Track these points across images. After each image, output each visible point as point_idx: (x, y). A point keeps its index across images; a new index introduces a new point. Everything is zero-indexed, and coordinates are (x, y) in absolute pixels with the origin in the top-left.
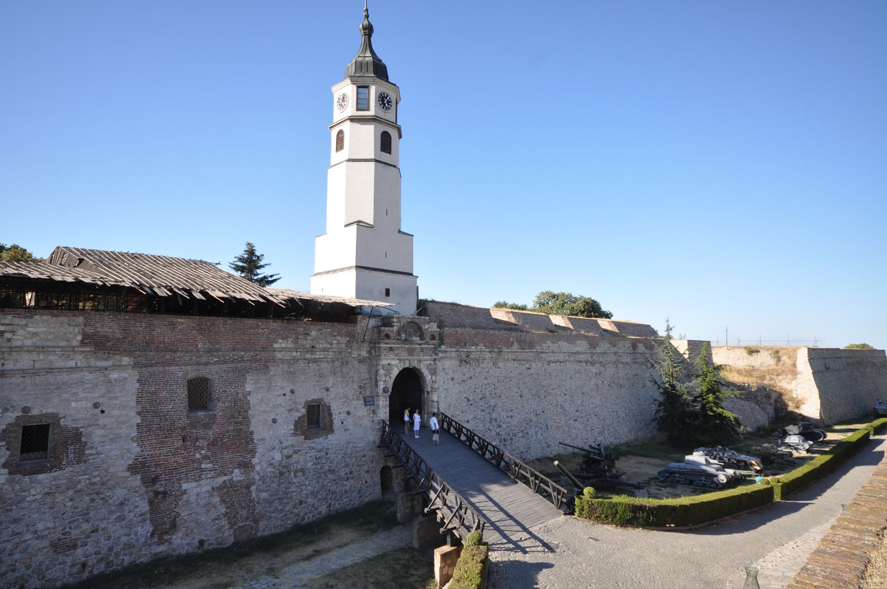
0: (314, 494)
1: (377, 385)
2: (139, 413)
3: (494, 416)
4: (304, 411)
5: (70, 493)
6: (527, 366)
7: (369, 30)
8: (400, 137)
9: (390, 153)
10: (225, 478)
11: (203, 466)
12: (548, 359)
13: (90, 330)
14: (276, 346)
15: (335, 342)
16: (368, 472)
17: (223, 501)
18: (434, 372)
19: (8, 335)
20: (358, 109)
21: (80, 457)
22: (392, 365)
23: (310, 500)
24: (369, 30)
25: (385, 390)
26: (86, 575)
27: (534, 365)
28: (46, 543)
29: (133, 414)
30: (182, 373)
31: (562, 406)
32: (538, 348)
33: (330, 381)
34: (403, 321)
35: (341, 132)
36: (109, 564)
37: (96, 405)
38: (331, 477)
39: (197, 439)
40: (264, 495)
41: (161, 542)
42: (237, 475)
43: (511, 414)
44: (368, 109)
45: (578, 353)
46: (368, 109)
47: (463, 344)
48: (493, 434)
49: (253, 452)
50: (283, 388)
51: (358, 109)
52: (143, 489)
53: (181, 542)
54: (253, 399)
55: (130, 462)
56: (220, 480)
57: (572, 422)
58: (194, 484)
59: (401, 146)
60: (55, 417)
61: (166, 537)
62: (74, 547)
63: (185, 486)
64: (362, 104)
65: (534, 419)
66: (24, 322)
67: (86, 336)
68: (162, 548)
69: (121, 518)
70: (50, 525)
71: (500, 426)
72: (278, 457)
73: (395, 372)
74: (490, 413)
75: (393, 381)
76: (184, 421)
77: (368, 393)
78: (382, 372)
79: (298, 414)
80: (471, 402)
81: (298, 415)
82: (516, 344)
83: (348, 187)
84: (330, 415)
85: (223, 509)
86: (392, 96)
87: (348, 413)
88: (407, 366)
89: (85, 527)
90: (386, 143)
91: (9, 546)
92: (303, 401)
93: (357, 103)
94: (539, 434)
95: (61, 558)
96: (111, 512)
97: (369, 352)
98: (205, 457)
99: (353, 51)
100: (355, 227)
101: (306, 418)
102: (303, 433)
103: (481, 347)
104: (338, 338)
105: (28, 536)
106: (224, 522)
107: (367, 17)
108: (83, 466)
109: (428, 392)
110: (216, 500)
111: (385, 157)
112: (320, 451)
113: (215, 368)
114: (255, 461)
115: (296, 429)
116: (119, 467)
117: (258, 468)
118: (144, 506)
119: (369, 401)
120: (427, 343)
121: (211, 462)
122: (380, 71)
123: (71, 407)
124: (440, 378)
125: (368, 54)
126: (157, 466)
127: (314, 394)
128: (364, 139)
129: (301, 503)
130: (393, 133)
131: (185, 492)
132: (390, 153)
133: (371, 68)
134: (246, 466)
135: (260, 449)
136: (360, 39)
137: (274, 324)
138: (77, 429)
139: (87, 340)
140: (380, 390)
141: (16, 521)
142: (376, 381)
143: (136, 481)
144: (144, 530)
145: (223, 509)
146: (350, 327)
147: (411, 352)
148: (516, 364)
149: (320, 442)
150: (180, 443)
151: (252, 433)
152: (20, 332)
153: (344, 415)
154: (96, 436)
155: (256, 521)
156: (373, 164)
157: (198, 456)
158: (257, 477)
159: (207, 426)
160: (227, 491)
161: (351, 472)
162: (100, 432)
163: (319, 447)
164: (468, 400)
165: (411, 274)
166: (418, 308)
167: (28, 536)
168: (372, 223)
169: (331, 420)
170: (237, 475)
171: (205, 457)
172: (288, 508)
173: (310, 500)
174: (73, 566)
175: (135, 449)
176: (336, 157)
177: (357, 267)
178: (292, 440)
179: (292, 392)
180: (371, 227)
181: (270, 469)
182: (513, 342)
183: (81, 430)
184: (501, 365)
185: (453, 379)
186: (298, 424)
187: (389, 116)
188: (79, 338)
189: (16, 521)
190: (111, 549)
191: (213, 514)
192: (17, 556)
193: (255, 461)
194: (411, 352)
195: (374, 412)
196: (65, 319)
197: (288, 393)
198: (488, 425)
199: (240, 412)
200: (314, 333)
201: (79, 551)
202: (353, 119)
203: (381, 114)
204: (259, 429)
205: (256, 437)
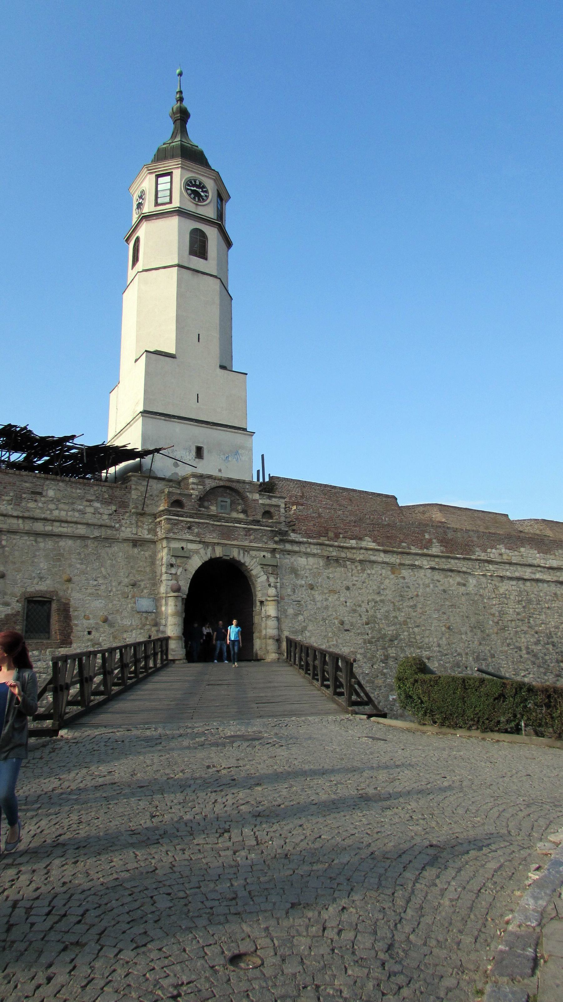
4: (17, 606)
6: (459, 579)
9: (206, 259)
15: (90, 510)
20: (157, 204)
34: (210, 484)
44: (171, 202)
47: (331, 534)
73: (196, 563)
74: (384, 648)
75: (190, 576)
79: (8, 610)
80: (347, 627)
88: (219, 552)
92: (18, 591)
101: (19, 618)
104: (97, 505)
109: (262, 602)
111: (197, 263)
120: (257, 522)
132: (206, 259)
147: (227, 533)
164: (342, 623)
168: (172, 351)
176: (131, 273)
177: (145, 413)
182: (430, 541)
194: (227, 533)
203: (190, 207)
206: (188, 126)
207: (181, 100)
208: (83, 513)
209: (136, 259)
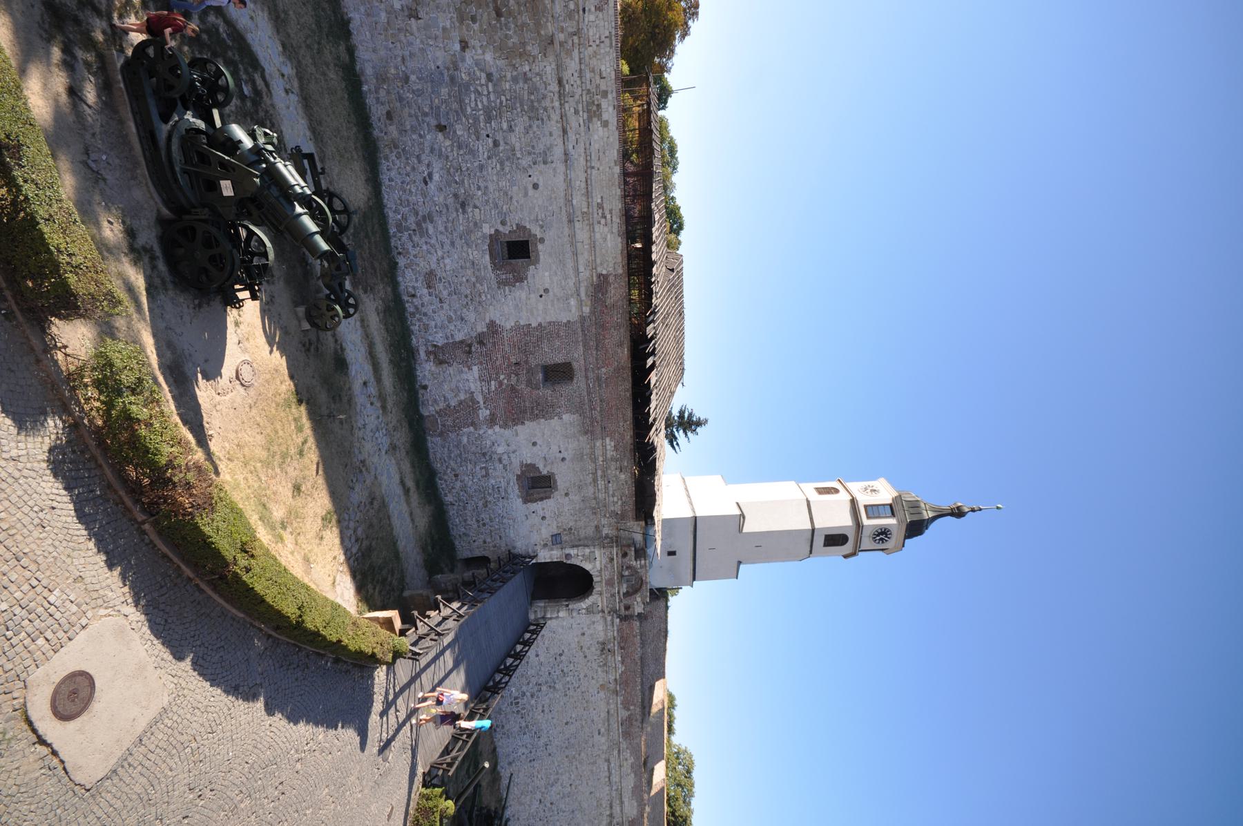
0: (464, 488)
1: (573, 547)
2: (540, 325)
3: (544, 688)
4: (545, 472)
5: (473, 279)
6: (603, 730)
7: (958, 513)
8: (845, 557)
9: (825, 545)
12: (612, 760)
13: (611, 279)
14: (608, 440)
16: (485, 542)
17: (461, 403)
18: (589, 611)
19: (603, 221)
20: (866, 507)
21: (502, 284)
22: (595, 562)
23: (458, 484)
24: (958, 513)
25: (568, 556)
26: (405, 298)
27: (603, 740)
28: (434, 266)
29: (539, 320)
30: (577, 356)
31: (557, 781)
32: (624, 745)
33: (575, 498)
34: (641, 572)
35: (837, 491)
36: (413, 314)
37: (546, 291)
38: (480, 504)
39: (517, 375)
40: (465, 440)
41: (428, 353)
42: (484, 413)
43: (547, 710)
44: (868, 517)
45: (622, 802)
46: (868, 517)
48: (524, 688)
49: (505, 426)
50: (566, 450)
51: (866, 507)
52: (474, 335)
53: (426, 370)
54: (555, 422)
56: (480, 399)
57: (538, 796)
58: (477, 376)
59: (833, 558)
60: (537, 261)
61: (432, 357)
62: (429, 287)
63: (475, 368)
64: (872, 510)
65: (542, 741)
66: (615, 230)
67: (606, 277)
68: (422, 355)
69: (450, 320)
70: (448, 268)
71: (532, 696)
72: (500, 450)
73: (587, 566)
76: (533, 362)
77: (565, 538)
78: (587, 551)
81: (541, 467)
82: (627, 714)
83: (778, 505)
84: (542, 499)
85: (453, 404)
86: (890, 544)
87: (543, 518)
88: (595, 579)
89: (445, 293)
90: (835, 540)
91: (433, 241)
92: (555, 471)
93: (872, 506)
94: (524, 750)
95: (421, 279)
96: (455, 311)
97: (607, 537)
98: (501, 383)
99: (931, 498)
100: (738, 513)
102: (523, 472)
103: (621, 668)
105: (440, 253)
106: (442, 405)
107: (973, 510)
108: (495, 286)
110: (462, 397)
111: (819, 540)
112: (506, 491)
113: (583, 385)
114: (497, 428)
115: (527, 465)
116: (493, 314)
117: (490, 432)
118: (459, 337)
119: (556, 540)
120: (621, 601)
122: (916, 528)
123: (544, 272)
124: (584, 619)
125: (931, 514)
126: (494, 344)
127: (562, 482)
128: (835, 516)
129: (456, 476)
130: (847, 548)
131: (470, 369)
132: (825, 545)
133: (915, 518)
134: (492, 421)
135: (507, 432)
136: (946, 504)
137: (628, 436)
140: (567, 551)
141: (453, 244)
142: (577, 546)
143: (481, 328)
144: (439, 339)
145: (453, 404)
146: (631, 514)
147: (610, 583)
148: (604, 715)
149: (514, 491)
150: (513, 360)
152: (606, 229)
153: (541, 513)
154: (520, 293)
155: (441, 434)
156: (810, 527)
157: (502, 377)
158: (481, 432)
159: (529, 383)
160: (470, 405)
161: (484, 525)
162: (524, 296)
163: (510, 490)
165: (694, 579)
166: (659, 590)
167: (440, 253)
169: (536, 501)
170: (484, 413)
171: (501, 383)
172: (452, 463)
173: (458, 484)
174: (414, 288)
175: (509, 325)
176: (809, 489)
178: (516, 463)
179: (563, 459)
180: (740, 530)
181: (489, 443)
184: (602, 694)
185: (583, 634)
186: (532, 467)
187: (866, 543)
188: (604, 272)
189: (453, 244)
190: (425, 314)
191: (449, 395)
192: (425, 247)
193: (497, 428)
194: (610, 583)
195: (545, 545)
196: (619, 259)
197: (561, 456)
198: (534, 681)
199: (542, 411)
200: (623, 476)
201: (425, 291)
202: (853, 502)
203: (866, 533)
204: (526, 431)
205: (519, 428)
206: (949, 517)
209: (822, 491)
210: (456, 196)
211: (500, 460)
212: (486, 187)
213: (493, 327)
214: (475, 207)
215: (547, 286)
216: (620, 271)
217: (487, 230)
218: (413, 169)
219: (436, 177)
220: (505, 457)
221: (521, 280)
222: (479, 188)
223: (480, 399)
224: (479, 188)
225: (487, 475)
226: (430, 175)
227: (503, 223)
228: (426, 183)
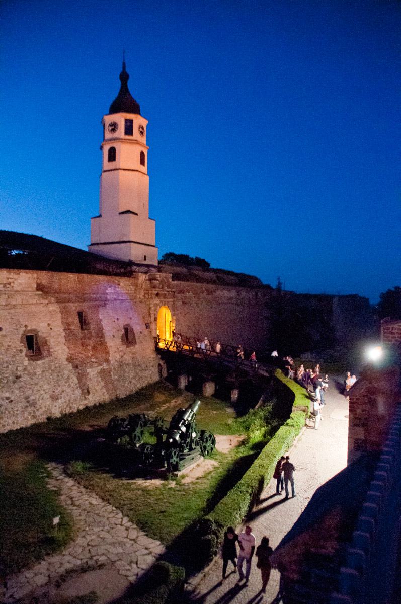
10: (101, 367)
11: (92, 360)
19: (12, 284)
21: (49, 354)
24: (124, 77)
29: (62, 330)
39: (87, 346)
40: (116, 377)
49: (108, 353)
55: (66, 357)
56: (100, 368)
60: (35, 330)
66: (16, 276)
68: (86, 402)
105: (42, 392)
110: (100, 379)
114: (110, 358)
118: (76, 381)
121: (95, 358)
123: (40, 326)
134: (107, 361)
138: (45, 338)
139: (40, 287)
141: (36, 384)
143: (70, 367)
151: (106, 343)
152: (16, 282)
179: (118, 319)
183: (47, 338)
188: (35, 286)
192: (41, 401)
196: (30, 275)
197: (116, 321)
207: (124, 68)
208: (128, 291)
210: (14, 382)
211: (122, 357)
212: (6, 362)
213: (70, 360)
214: (17, 369)
215: (46, 325)
216: (35, 275)
217: (26, 362)
218: (6, 409)
219: (7, 395)
220: (120, 354)
221: (46, 341)
222: (7, 367)
223: (100, 368)
224: (7, 367)
225: (128, 365)
226: (7, 398)
227: (21, 351)
228: (11, 401)
